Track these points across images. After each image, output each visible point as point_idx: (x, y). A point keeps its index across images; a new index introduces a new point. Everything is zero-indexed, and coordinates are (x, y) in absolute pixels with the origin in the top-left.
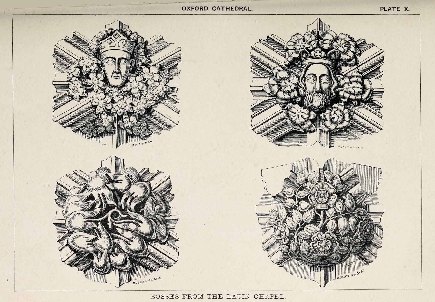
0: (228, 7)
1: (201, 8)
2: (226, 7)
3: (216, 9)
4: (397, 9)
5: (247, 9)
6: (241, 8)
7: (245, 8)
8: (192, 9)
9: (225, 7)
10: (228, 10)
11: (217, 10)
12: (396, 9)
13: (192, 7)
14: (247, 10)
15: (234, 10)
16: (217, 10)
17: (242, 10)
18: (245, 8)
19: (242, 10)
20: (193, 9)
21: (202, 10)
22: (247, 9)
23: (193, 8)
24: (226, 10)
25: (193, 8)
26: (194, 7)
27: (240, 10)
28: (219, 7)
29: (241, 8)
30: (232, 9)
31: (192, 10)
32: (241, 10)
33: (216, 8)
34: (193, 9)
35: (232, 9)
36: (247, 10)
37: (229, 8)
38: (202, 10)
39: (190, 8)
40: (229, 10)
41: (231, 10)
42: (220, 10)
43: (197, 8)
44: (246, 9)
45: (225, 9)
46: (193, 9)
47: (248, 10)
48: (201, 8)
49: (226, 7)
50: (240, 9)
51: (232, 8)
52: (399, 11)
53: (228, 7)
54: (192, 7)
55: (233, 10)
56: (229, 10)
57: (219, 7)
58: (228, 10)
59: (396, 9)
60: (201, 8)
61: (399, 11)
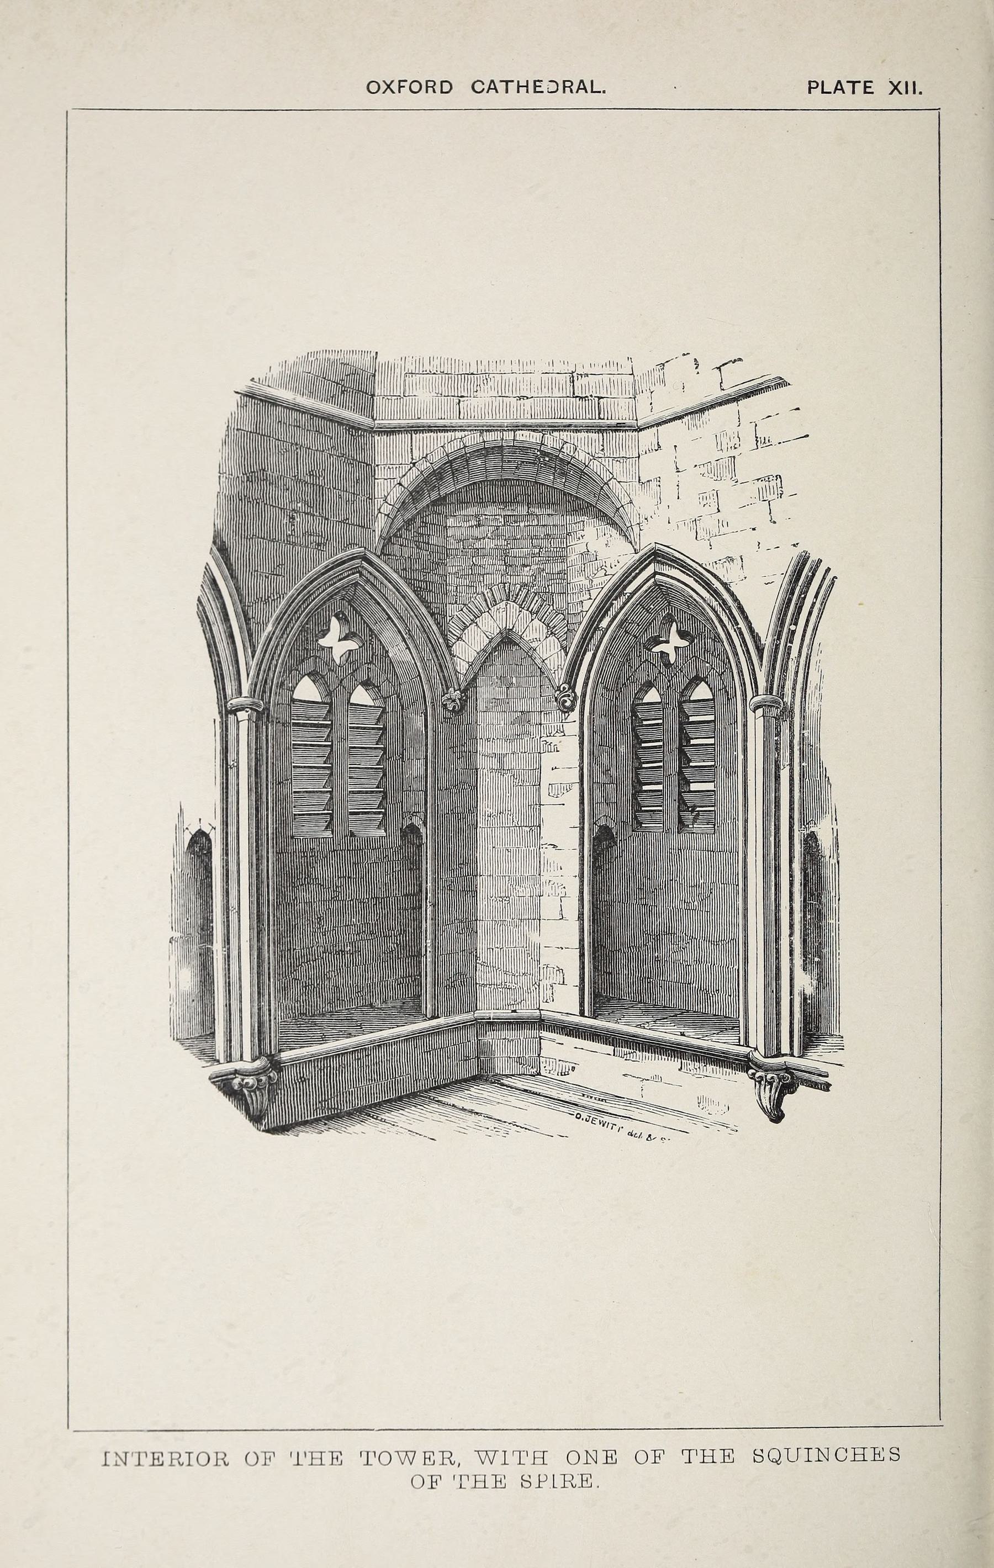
0: (523, 83)
1: (429, 86)
2: (518, 82)
3: (483, 89)
4: (865, 87)
5: (589, 89)
6: (568, 84)
7: (582, 86)
8: (400, 87)
9: (516, 83)
10: (523, 90)
11: (488, 92)
12: (859, 87)
13: (400, 81)
14: (586, 92)
15: (546, 92)
16: (488, 92)
17: (571, 91)
18: (582, 86)
19: (571, 91)
20: (404, 87)
21: (434, 91)
22: (589, 89)
23: (402, 84)
24: (518, 92)
25: (402, 84)
26: (405, 81)
27: (564, 92)
28: (492, 81)
29: (566, 86)
30: (538, 89)
31: (399, 92)
32: (568, 90)
33: (483, 87)
34: (404, 87)
35: (538, 89)
36: (586, 92)
37: (527, 86)
38: (434, 91)
39: (395, 87)
40: (527, 92)
41: (535, 92)
42: (497, 92)
43: (415, 87)
44: (585, 89)
45: (512, 87)
46: (401, 89)
47: (592, 92)
48: (431, 84)
49: (518, 82)
50: (564, 87)
51: (538, 84)
52: (872, 93)
53: (523, 83)
54: (400, 81)
55: (542, 92)
56: (527, 92)
57: (492, 81)
58: (523, 90)
59: (859, 87)
60: (431, 84)
61: (872, 93)
